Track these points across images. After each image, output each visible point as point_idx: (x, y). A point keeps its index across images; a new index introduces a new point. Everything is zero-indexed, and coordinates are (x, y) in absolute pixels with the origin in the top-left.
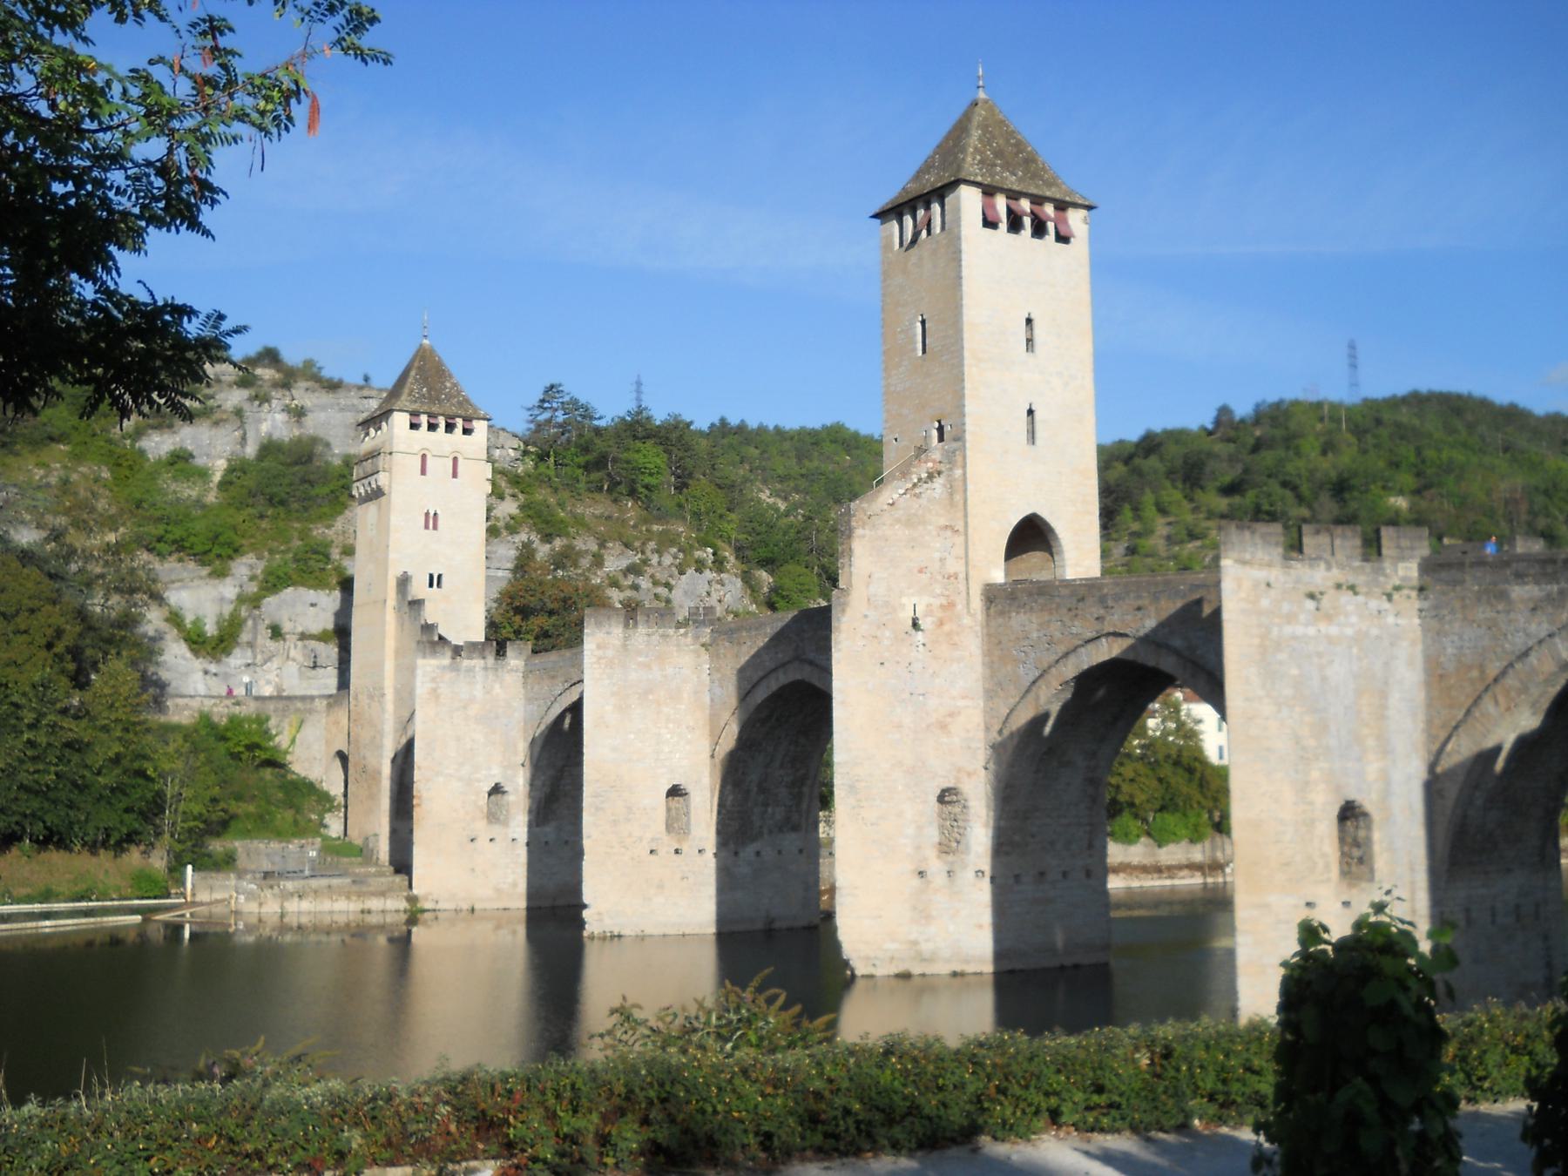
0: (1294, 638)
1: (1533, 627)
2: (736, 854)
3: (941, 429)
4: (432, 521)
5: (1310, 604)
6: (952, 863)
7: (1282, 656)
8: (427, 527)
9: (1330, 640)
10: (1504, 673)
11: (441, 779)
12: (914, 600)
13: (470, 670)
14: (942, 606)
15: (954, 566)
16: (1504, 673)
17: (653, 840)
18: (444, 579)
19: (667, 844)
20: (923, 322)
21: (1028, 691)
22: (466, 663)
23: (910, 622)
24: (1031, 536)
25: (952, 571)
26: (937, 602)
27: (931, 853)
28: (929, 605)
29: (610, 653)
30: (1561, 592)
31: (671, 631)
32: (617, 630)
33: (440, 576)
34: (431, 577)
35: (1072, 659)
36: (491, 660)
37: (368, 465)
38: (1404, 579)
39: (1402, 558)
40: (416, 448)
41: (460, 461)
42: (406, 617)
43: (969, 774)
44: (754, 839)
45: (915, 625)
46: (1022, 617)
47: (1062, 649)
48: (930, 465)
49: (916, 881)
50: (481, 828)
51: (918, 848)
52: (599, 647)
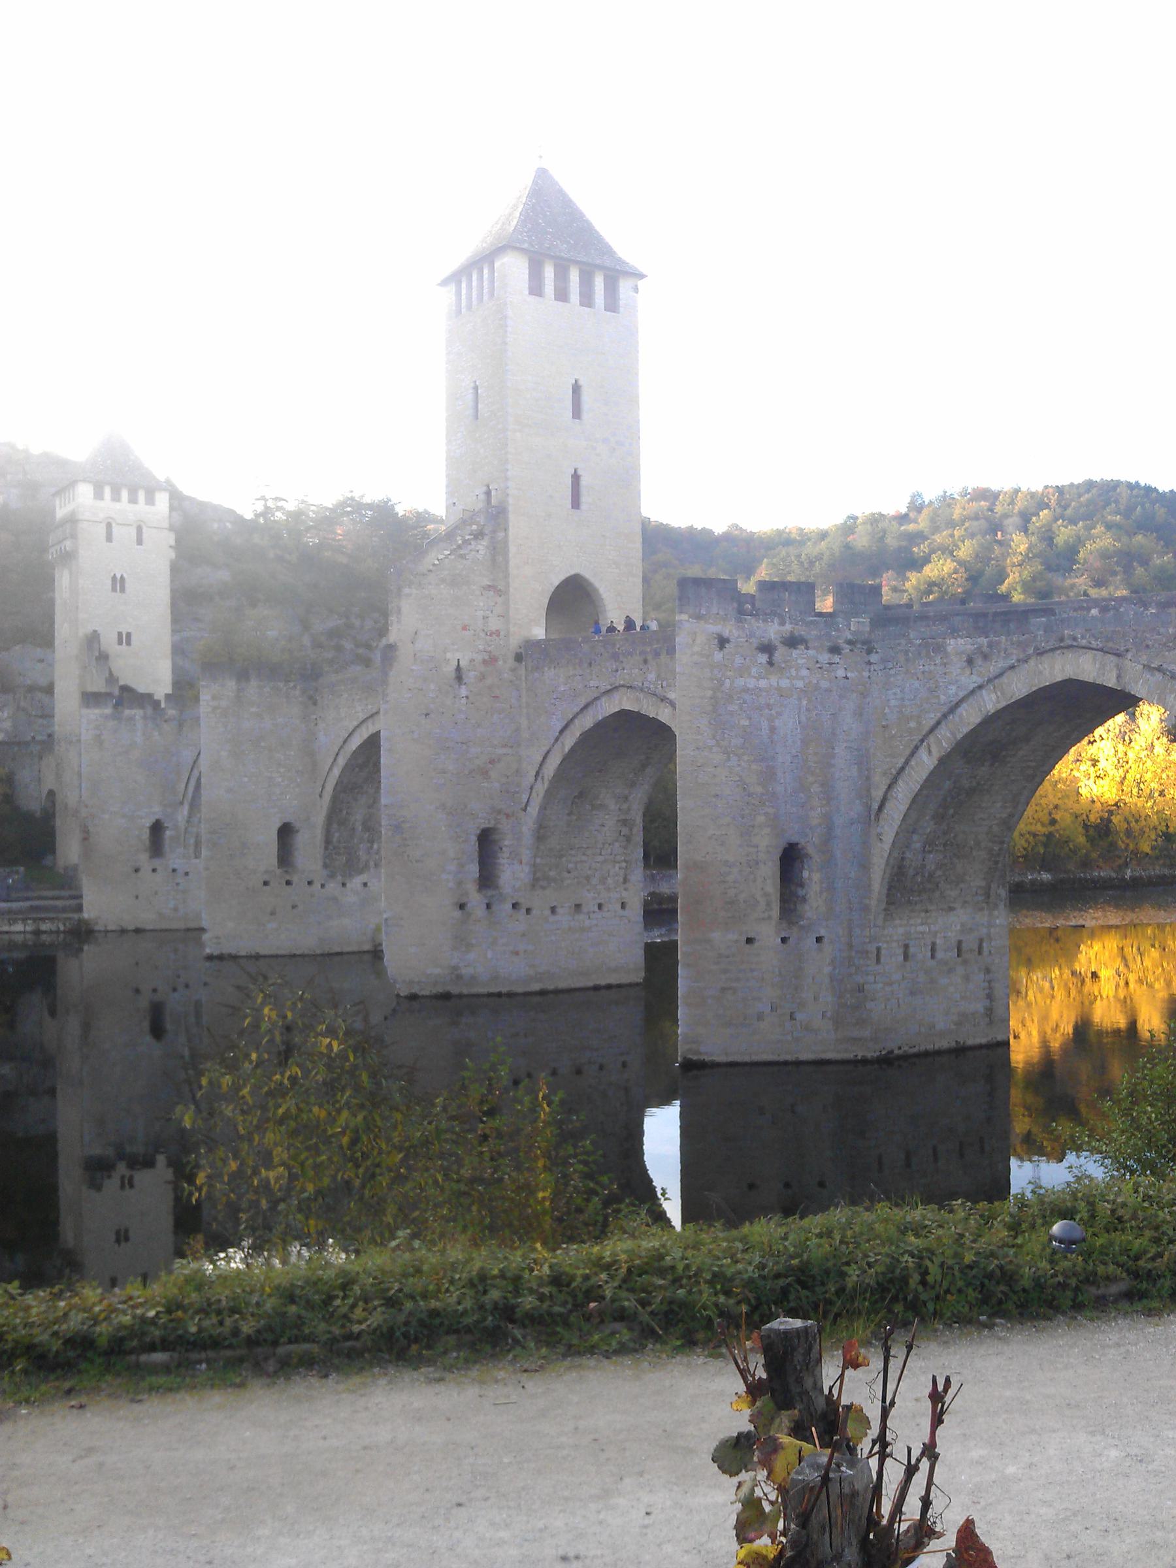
0: (746, 690)
1: (964, 679)
2: (344, 885)
3: (488, 493)
5: (763, 658)
6: (492, 896)
7: (733, 707)
8: (114, 589)
9: (781, 693)
10: (938, 723)
11: (107, 816)
12: (458, 655)
13: (131, 719)
14: (484, 662)
15: (494, 624)
16: (938, 723)
17: (266, 872)
18: (133, 638)
21: (557, 739)
22: (127, 712)
23: (453, 675)
25: (494, 629)
26: (479, 658)
27: (471, 888)
28: (472, 660)
29: (224, 703)
30: (990, 645)
31: (281, 685)
32: (231, 684)
33: (129, 635)
34: (120, 634)
35: (590, 711)
36: (149, 711)
38: (854, 633)
39: (856, 614)
41: (144, 529)
43: (508, 816)
44: (361, 872)
47: (582, 701)
48: (474, 527)
49: (457, 914)
50: (143, 858)
51: (460, 884)
52: (214, 698)
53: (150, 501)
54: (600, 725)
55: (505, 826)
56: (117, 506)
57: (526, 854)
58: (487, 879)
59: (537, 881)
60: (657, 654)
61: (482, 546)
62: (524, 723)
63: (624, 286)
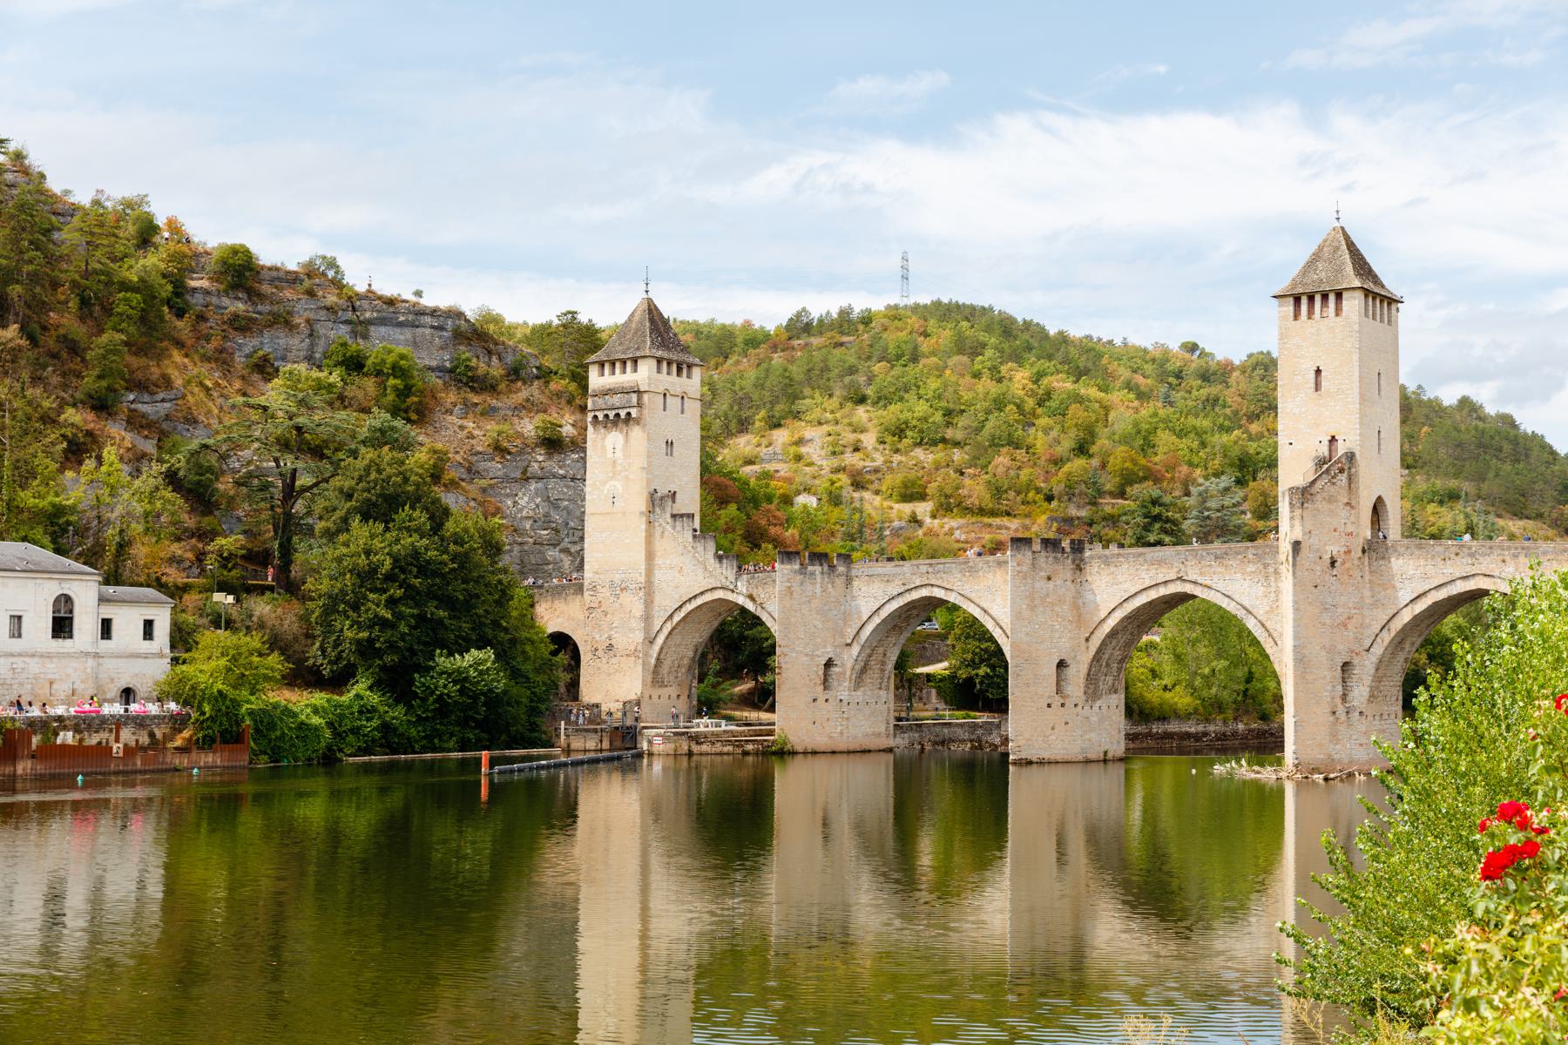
3: (1333, 439)
4: (670, 444)
13: (812, 574)
15: (1350, 528)
19: (1057, 700)
20: (1318, 371)
22: (810, 568)
24: (1378, 509)
27: (1338, 701)
29: (1025, 569)
36: (826, 568)
37: (616, 400)
40: (661, 390)
42: (669, 527)
45: (1333, 563)
46: (1400, 561)
53: (689, 377)
54: (1450, 599)
55: (1356, 661)
56: (670, 378)
57: (1368, 680)
58: (1344, 697)
59: (1372, 697)
60: (1515, 556)
61: (1344, 477)
62: (1367, 593)
63: (1394, 307)
